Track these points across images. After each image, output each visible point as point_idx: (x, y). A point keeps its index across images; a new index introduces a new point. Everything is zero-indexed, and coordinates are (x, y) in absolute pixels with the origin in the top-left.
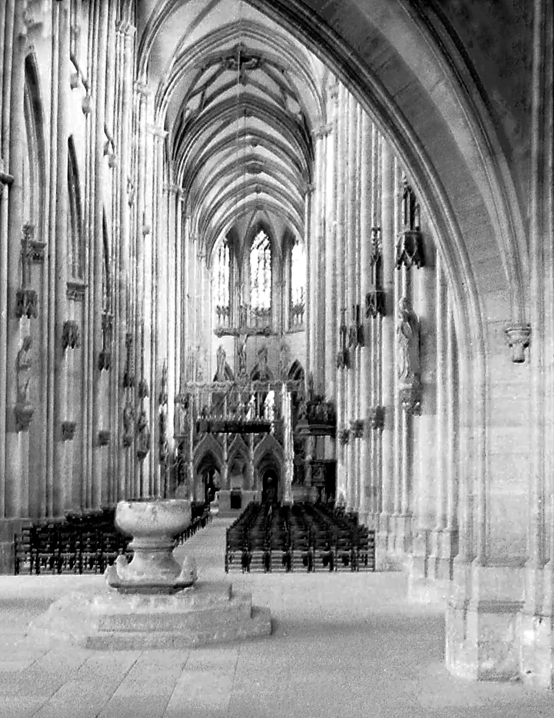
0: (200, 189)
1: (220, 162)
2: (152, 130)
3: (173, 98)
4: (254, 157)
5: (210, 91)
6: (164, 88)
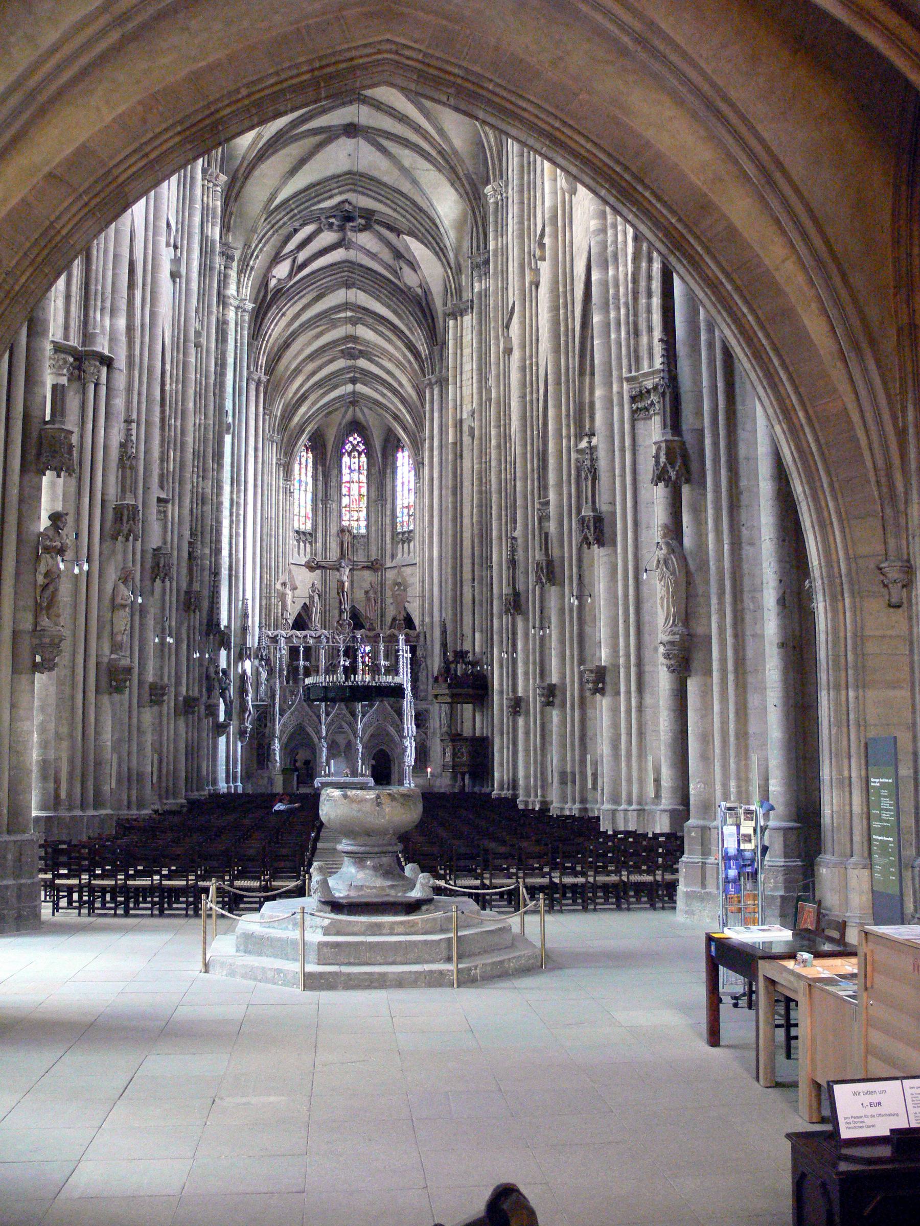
1: (309, 343)
4: (354, 339)
6: (249, 252)
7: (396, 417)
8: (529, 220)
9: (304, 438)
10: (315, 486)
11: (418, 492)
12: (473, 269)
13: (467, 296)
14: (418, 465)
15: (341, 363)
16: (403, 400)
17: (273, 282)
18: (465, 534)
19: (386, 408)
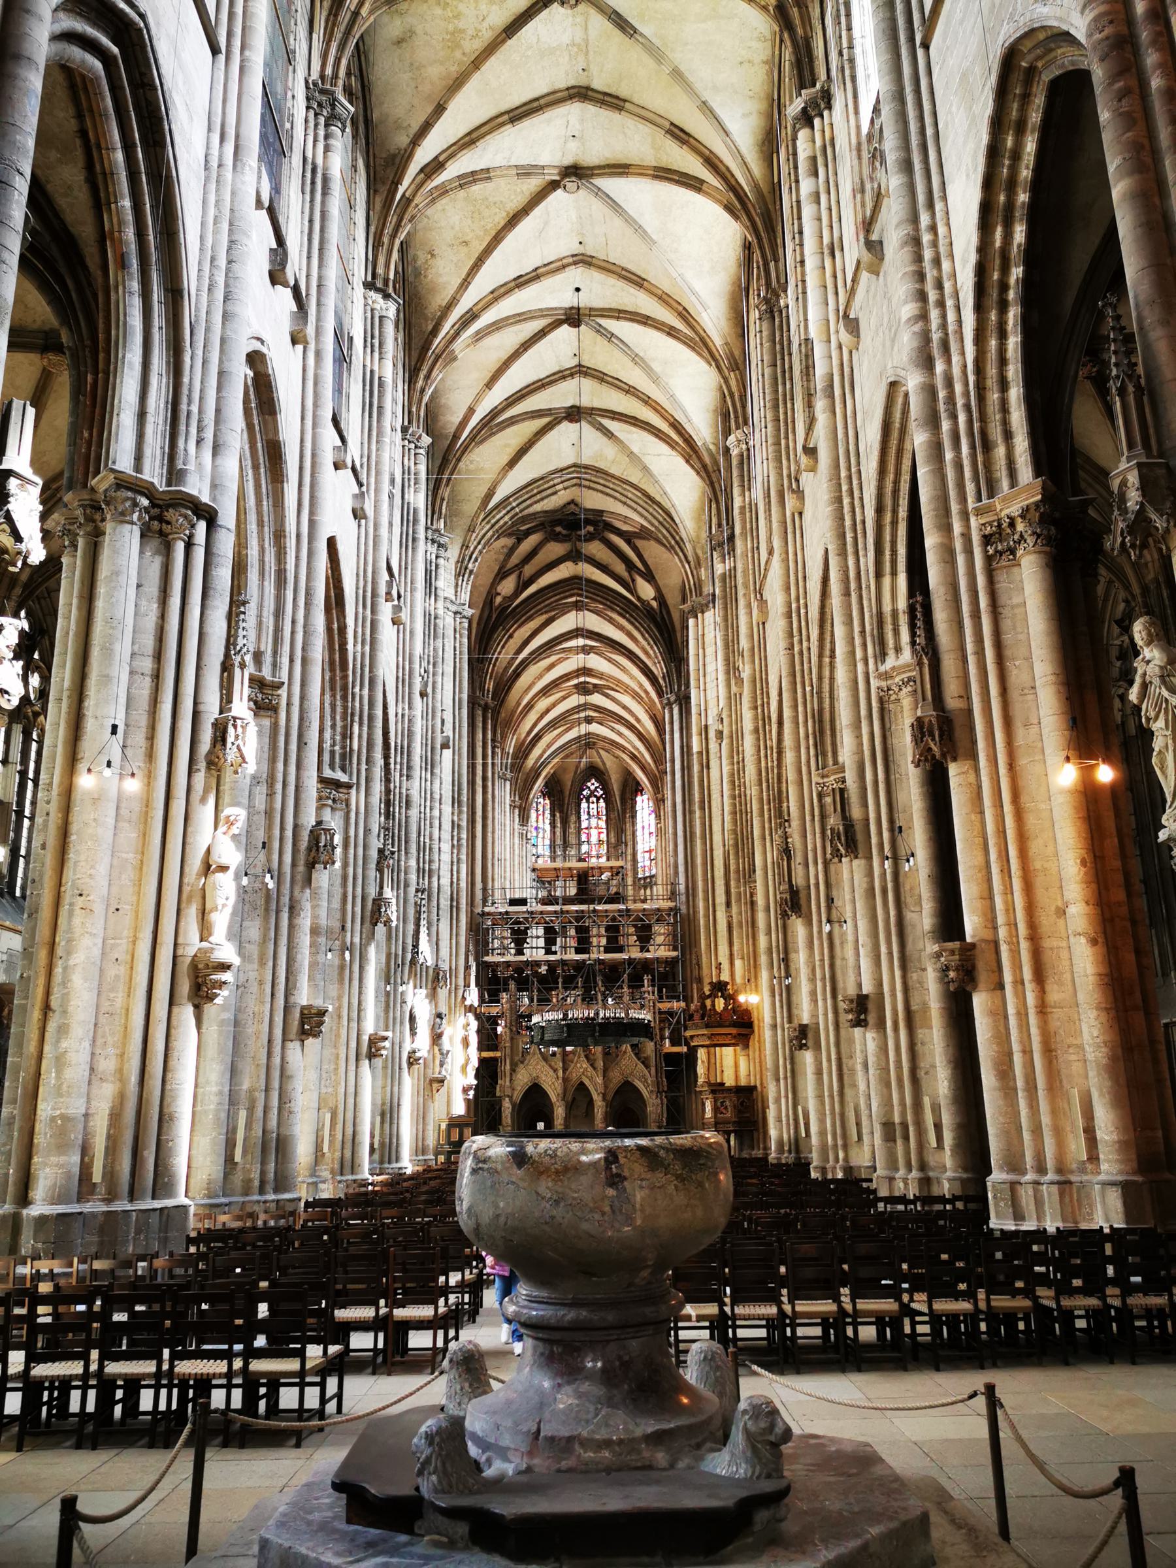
0: (514, 712)
1: (540, 676)
2: (452, 600)
3: (484, 563)
4: (586, 671)
5: (528, 570)
6: (468, 553)
7: (634, 757)
8: (787, 438)
9: (539, 784)
10: (553, 833)
11: (660, 832)
12: (713, 549)
13: (707, 589)
14: (659, 802)
15: (575, 700)
16: (641, 736)
17: (498, 600)
18: (716, 853)
19: (623, 749)
